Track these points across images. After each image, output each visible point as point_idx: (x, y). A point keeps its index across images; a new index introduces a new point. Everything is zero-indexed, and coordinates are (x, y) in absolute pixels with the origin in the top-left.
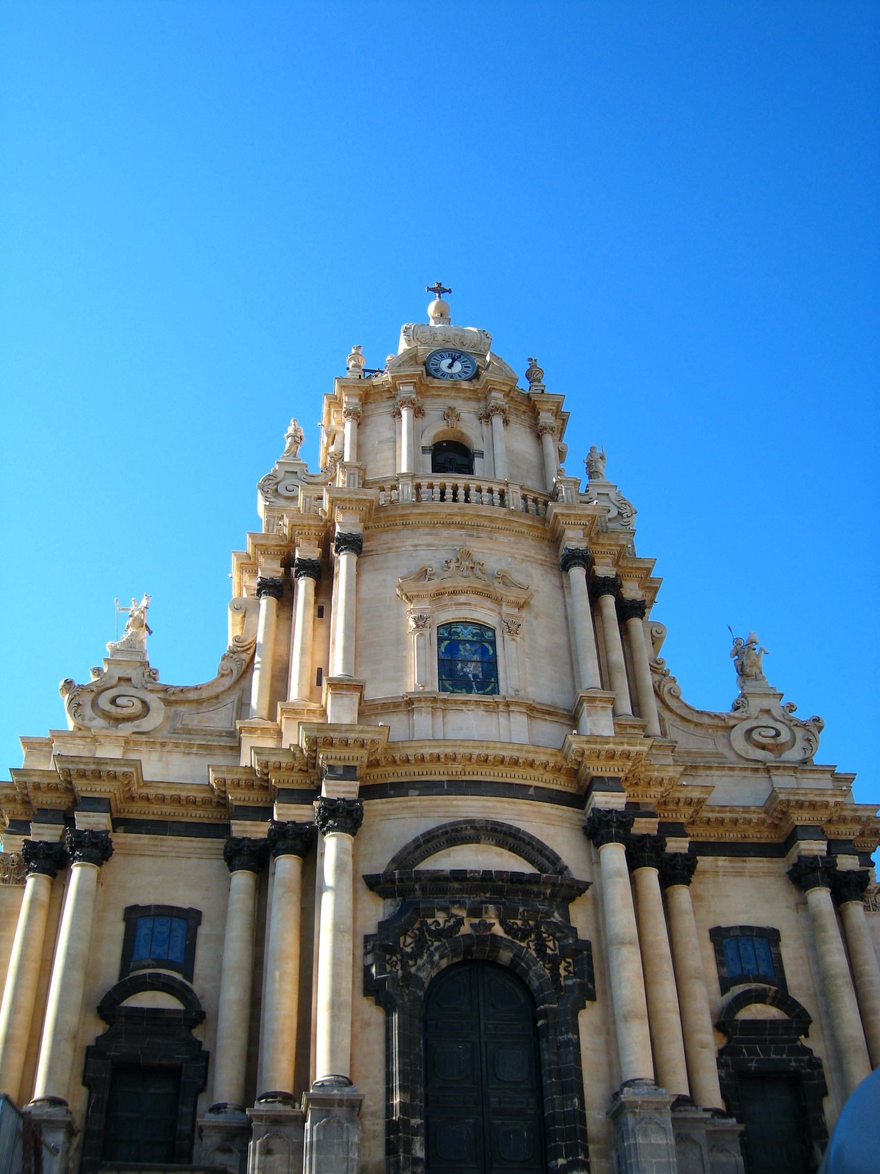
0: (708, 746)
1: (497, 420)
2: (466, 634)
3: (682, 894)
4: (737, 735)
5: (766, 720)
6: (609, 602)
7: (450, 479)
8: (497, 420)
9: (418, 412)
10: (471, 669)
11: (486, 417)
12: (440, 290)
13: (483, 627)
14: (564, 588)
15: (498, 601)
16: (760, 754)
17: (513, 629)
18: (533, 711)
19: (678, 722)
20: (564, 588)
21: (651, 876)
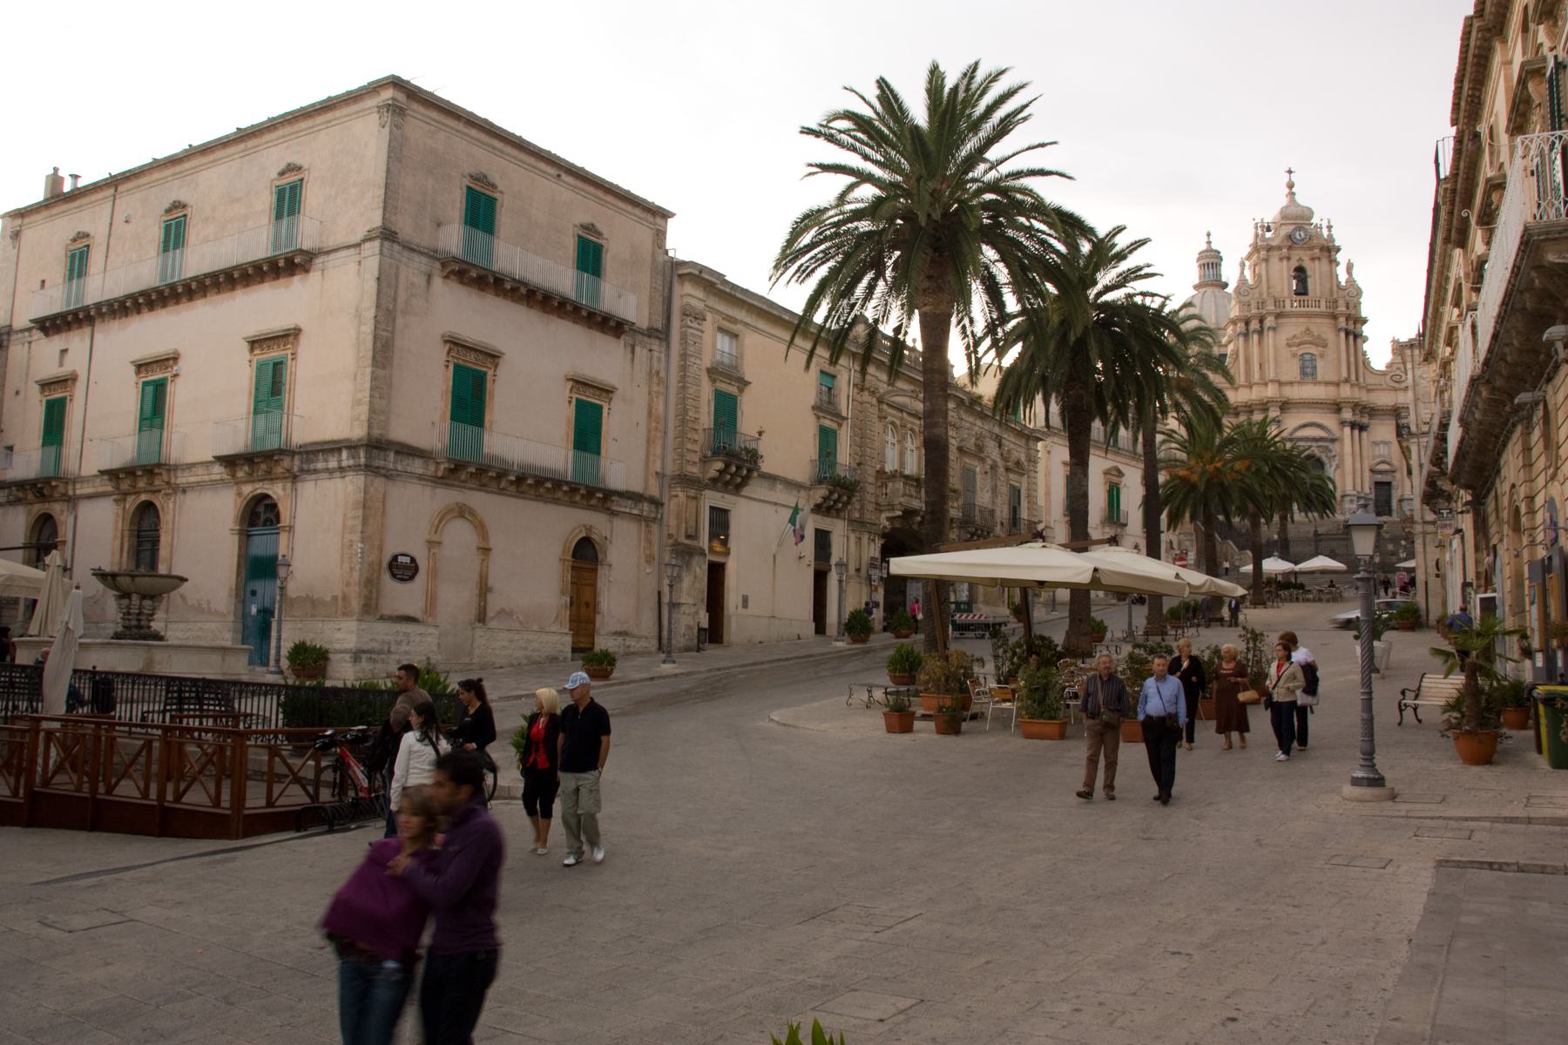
0: (1377, 382)
1: (1317, 262)
2: (1307, 357)
3: (1364, 434)
4: (1389, 377)
5: (1398, 372)
6: (1351, 338)
7: (1302, 298)
8: (1317, 262)
9: (1289, 258)
10: (1309, 370)
11: (1313, 259)
12: (1290, 172)
13: (1312, 355)
14: (1338, 336)
15: (1317, 345)
16: (1394, 384)
17: (1322, 356)
18: (1327, 384)
19: (1370, 375)
20: (1338, 336)
21: (1356, 432)
